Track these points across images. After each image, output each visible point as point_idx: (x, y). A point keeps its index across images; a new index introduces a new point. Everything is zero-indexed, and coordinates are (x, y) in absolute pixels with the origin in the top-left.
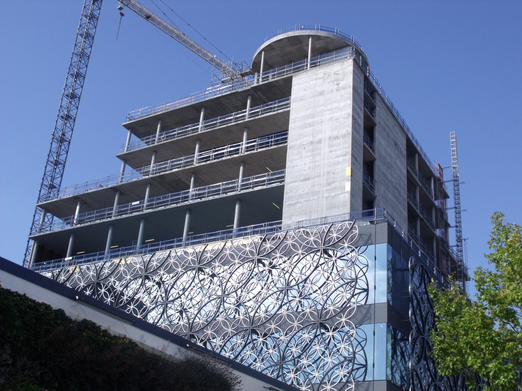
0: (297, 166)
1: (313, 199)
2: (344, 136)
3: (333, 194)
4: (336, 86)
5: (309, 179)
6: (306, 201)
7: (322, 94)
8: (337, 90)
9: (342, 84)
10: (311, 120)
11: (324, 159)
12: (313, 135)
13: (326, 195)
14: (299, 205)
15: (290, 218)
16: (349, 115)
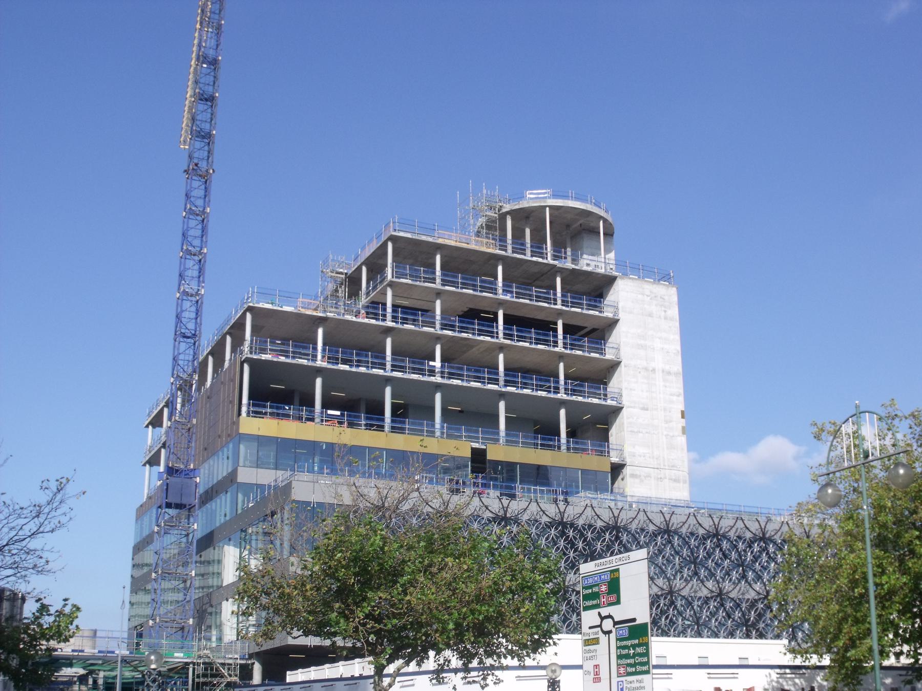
0: (634, 390)
1: (654, 434)
2: (676, 374)
3: (671, 434)
4: (663, 313)
5: (647, 410)
6: (647, 433)
7: (650, 315)
8: (666, 318)
9: (669, 312)
10: (642, 342)
11: (660, 393)
12: (646, 360)
13: (665, 433)
14: (641, 435)
15: (634, 447)
16: (678, 352)
